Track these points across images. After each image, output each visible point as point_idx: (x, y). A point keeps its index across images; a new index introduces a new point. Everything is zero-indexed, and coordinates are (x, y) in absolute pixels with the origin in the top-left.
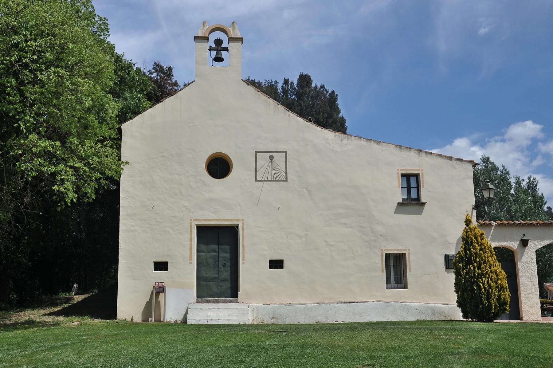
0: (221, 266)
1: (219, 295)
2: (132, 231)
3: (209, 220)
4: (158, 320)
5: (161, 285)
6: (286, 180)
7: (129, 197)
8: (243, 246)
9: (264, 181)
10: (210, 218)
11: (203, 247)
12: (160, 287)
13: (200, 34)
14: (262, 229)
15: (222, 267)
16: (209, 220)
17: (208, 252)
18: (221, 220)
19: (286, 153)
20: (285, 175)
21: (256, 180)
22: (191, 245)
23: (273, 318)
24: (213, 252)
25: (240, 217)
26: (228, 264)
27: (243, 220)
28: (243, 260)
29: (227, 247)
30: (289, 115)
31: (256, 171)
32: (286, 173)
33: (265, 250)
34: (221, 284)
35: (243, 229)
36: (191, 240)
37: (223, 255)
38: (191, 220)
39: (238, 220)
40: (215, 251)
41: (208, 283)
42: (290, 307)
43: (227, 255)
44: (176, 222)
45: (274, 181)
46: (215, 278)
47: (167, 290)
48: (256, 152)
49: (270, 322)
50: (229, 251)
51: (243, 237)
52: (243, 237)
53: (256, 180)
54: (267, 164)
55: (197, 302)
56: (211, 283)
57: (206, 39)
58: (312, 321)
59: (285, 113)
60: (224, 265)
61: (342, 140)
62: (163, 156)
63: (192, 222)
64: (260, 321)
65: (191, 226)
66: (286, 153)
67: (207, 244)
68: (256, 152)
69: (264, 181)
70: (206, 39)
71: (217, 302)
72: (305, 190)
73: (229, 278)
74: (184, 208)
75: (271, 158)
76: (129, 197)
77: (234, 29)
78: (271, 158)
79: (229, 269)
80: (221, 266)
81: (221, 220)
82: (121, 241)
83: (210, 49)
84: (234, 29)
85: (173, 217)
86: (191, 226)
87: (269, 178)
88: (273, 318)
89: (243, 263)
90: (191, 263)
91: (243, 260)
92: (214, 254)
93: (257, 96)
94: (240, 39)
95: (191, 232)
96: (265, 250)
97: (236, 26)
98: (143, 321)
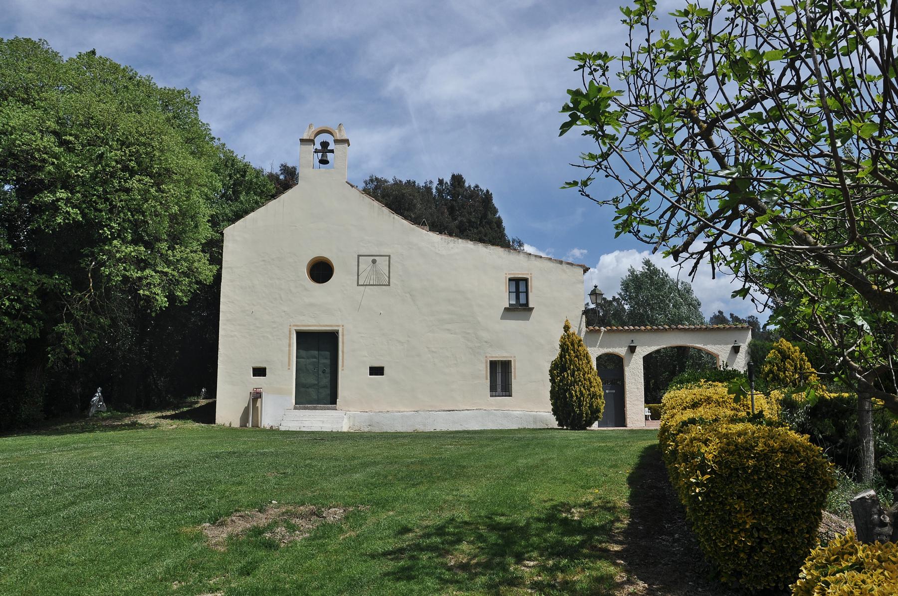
0: (320, 372)
1: (318, 401)
2: (232, 336)
3: (309, 326)
4: (256, 425)
5: (258, 390)
6: (389, 285)
7: (229, 301)
8: (343, 352)
9: (366, 285)
10: (310, 324)
11: (303, 353)
12: (257, 393)
13: (305, 137)
14: (363, 335)
15: (322, 374)
16: (309, 326)
17: (308, 358)
18: (321, 326)
19: (389, 256)
20: (387, 279)
21: (358, 285)
22: (289, 351)
23: (370, 425)
24: (313, 358)
25: (340, 323)
26: (328, 370)
27: (343, 326)
28: (343, 366)
29: (328, 353)
30: (394, 218)
31: (358, 276)
32: (389, 278)
33: (366, 356)
34: (321, 390)
35: (343, 335)
36: (290, 345)
37: (323, 361)
38: (290, 326)
39: (338, 326)
40: (315, 357)
41: (307, 390)
42: (387, 415)
43: (328, 362)
44: (275, 328)
45: (376, 285)
46: (315, 385)
47: (264, 395)
48: (359, 256)
49: (366, 430)
50: (329, 357)
51: (343, 343)
52: (343, 343)
53: (358, 285)
54: (370, 268)
55: (295, 408)
56: (310, 389)
57: (311, 141)
58: (410, 430)
59: (390, 216)
60: (324, 372)
61: (448, 243)
62: (264, 261)
63: (292, 327)
64: (357, 428)
65: (290, 331)
66: (389, 256)
67: (307, 349)
68: (359, 256)
69: (366, 285)
70: (311, 141)
71: (315, 409)
72: (408, 295)
73: (328, 385)
74: (283, 313)
75: (374, 262)
76: (229, 301)
77: (340, 130)
78: (374, 262)
79: (329, 375)
80: (320, 372)
81: (321, 326)
82: (220, 347)
83: (316, 151)
84: (340, 130)
85: (273, 322)
86: (290, 331)
87: (371, 283)
88: (370, 425)
89: (343, 370)
90: (289, 369)
91: (343, 366)
92: (314, 360)
93: (362, 198)
94: (346, 141)
95: (290, 338)
96: (366, 356)
97: (343, 128)
98: (241, 426)
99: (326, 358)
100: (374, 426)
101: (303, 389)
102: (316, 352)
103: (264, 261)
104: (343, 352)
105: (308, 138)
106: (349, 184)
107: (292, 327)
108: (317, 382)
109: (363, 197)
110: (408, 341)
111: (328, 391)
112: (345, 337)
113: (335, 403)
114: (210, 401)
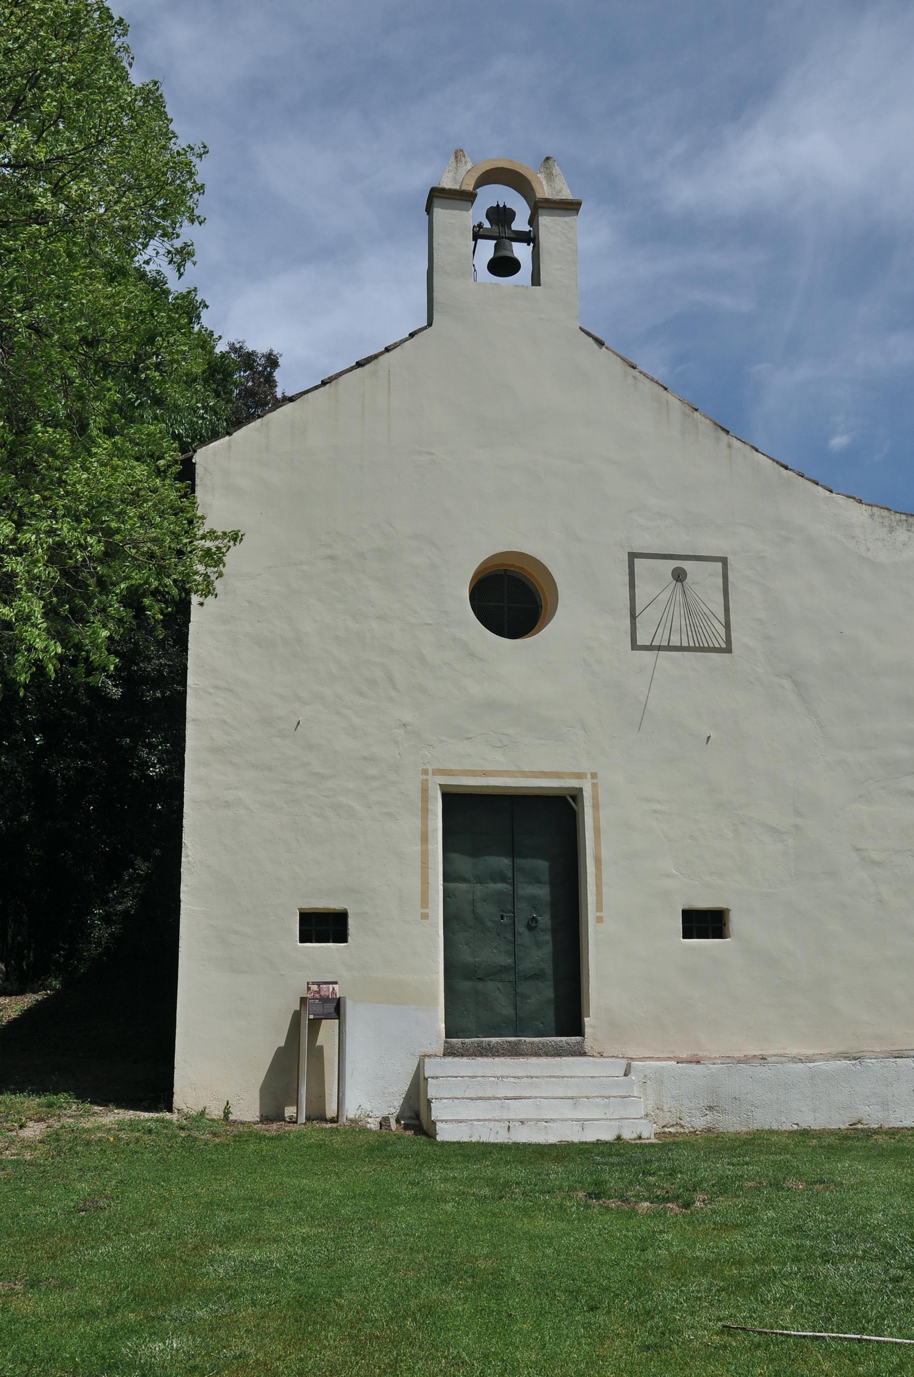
0: (521, 928)
1: (518, 1027)
2: (227, 804)
3: (485, 774)
4: (317, 1116)
5: (327, 990)
6: (728, 650)
7: (217, 688)
8: (598, 861)
9: (659, 648)
10: (488, 767)
11: (463, 863)
12: (325, 1000)
13: (447, 183)
14: (658, 807)
15: (526, 932)
16: (485, 774)
17: (480, 881)
18: (524, 774)
19: (724, 561)
20: (722, 631)
21: (635, 646)
22: (425, 854)
23: (711, 1108)
24: (494, 880)
25: (586, 766)
26: (545, 920)
27: (594, 776)
28: (599, 907)
29: (542, 865)
30: (729, 446)
31: (633, 617)
32: (727, 626)
33: (669, 876)
34: (524, 988)
35: (596, 807)
36: (425, 838)
37: (527, 890)
38: (425, 772)
39: (579, 776)
40: (503, 879)
41: (480, 986)
42: (764, 1072)
43: (543, 892)
44: (373, 778)
45: (688, 649)
46: (504, 969)
47: (351, 1011)
48: (632, 556)
49: (700, 1123)
50: (546, 877)
51: (597, 830)
52: (597, 830)
53: (635, 646)
54: (665, 596)
55: (450, 1052)
56: (491, 985)
57: (466, 197)
58: (839, 1121)
59: (718, 440)
60: (532, 926)
61: (891, 530)
62: (331, 558)
63: (430, 777)
64: (668, 1118)
65: (425, 791)
66: (724, 561)
67: (475, 853)
68: (632, 556)
69: (659, 648)
70: (466, 197)
71: (514, 1052)
72: (787, 683)
73: (548, 968)
74: (401, 731)
75: (679, 576)
76: (217, 688)
77: (550, 176)
78: (679, 576)
79: (548, 937)
80: (521, 928)
81: (524, 774)
82: (186, 839)
83: (478, 234)
84: (550, 176)
85: (365, 758)
86: (425, 791)
87: (675, 641)
88: (711, 1108)
89: (600, 920)
90: (425, 916)
91: (599, 907)
92: (500, 886)
93: (630, 380)
94: (571, 207)
95: (425, 812)
96: (669, 876)
97: (556, 170)
98: (266, 1119)
99: (538, 881)
100: (725, 1112)
101: (465, 985)
102: (503, 863)
103: (331, 558)
104: (598, 861)
105: (457, 187)
106: (589, 334)
107: (430, 777)
108: (510, 961)
109: (635, 378)
110: (796, 826)
111: (545, 992)
112: (602, 813)
113: (578, 1030)
114: (449, 1040)
